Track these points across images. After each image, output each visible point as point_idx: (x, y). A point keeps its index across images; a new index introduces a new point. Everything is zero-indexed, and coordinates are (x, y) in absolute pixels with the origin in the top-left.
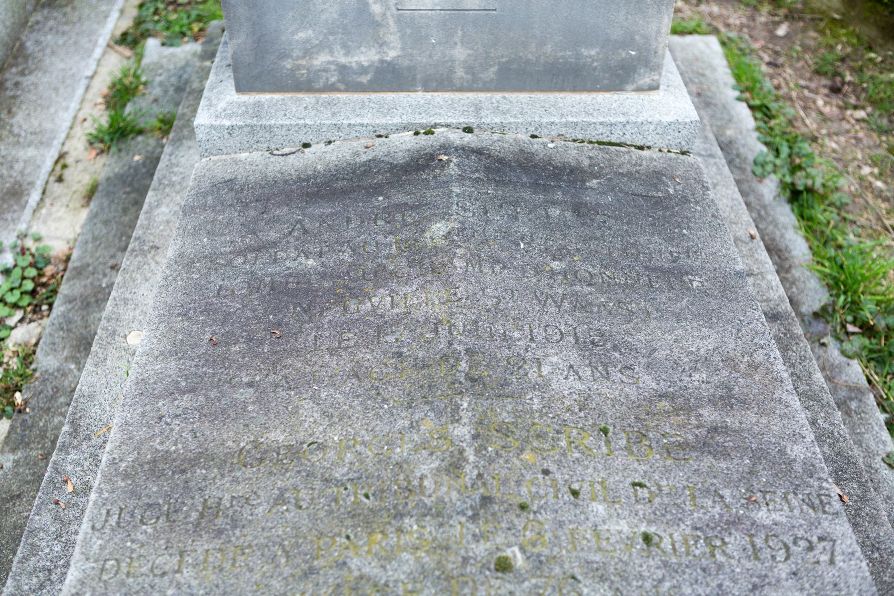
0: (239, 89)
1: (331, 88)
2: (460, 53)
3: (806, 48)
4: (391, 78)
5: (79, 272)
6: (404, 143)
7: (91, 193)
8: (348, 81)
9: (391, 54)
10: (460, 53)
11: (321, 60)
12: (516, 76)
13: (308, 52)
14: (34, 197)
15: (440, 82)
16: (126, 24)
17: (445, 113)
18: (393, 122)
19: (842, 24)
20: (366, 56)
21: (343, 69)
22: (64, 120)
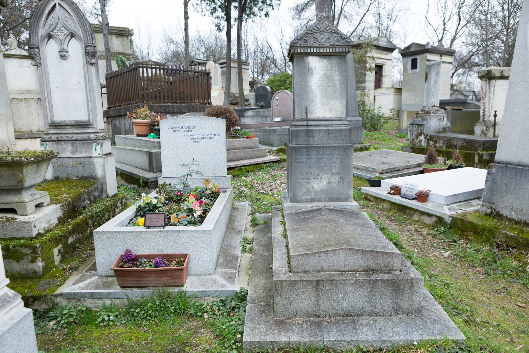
0: (291, 201)
1: (304, 202)
2: (323, 196)
3: (384, 215)
4: (313, 200)
5: (256, 239)
6: (316, 208)
7: (253, 232)
8: (307, 201)
9: (313, 197)
10: (323, 196)
11: (303, 197)
12: (331, 200)
13: (301, 196)
14: (243, 232)
15: (320, 201)
16: (250, 212)
17: (321, 204)
18: (314, 205)
19: (391, 210)
20: (309, 197)
21: (306, 199)
22: (244, 224)
